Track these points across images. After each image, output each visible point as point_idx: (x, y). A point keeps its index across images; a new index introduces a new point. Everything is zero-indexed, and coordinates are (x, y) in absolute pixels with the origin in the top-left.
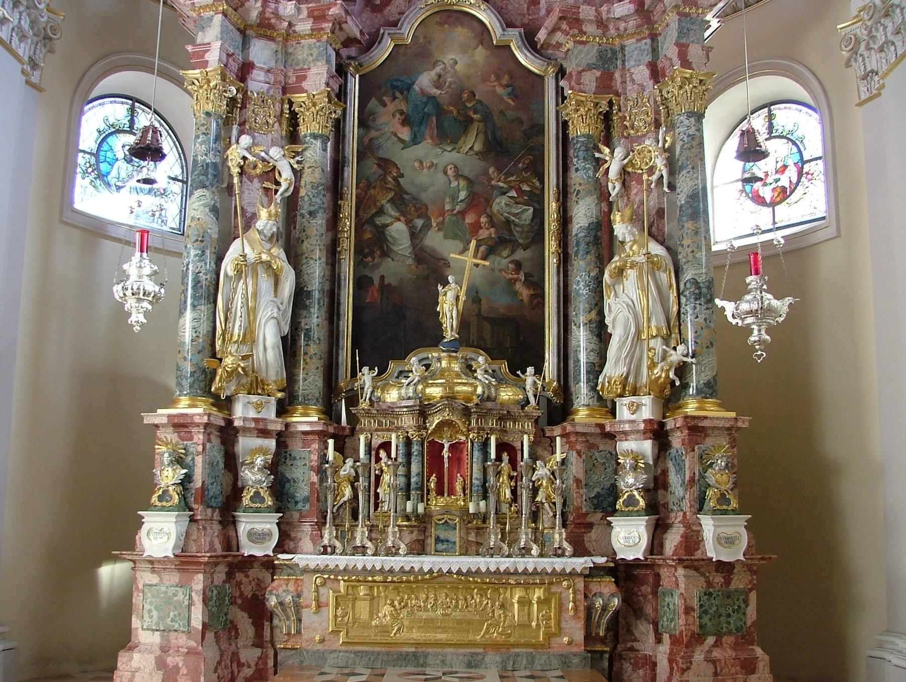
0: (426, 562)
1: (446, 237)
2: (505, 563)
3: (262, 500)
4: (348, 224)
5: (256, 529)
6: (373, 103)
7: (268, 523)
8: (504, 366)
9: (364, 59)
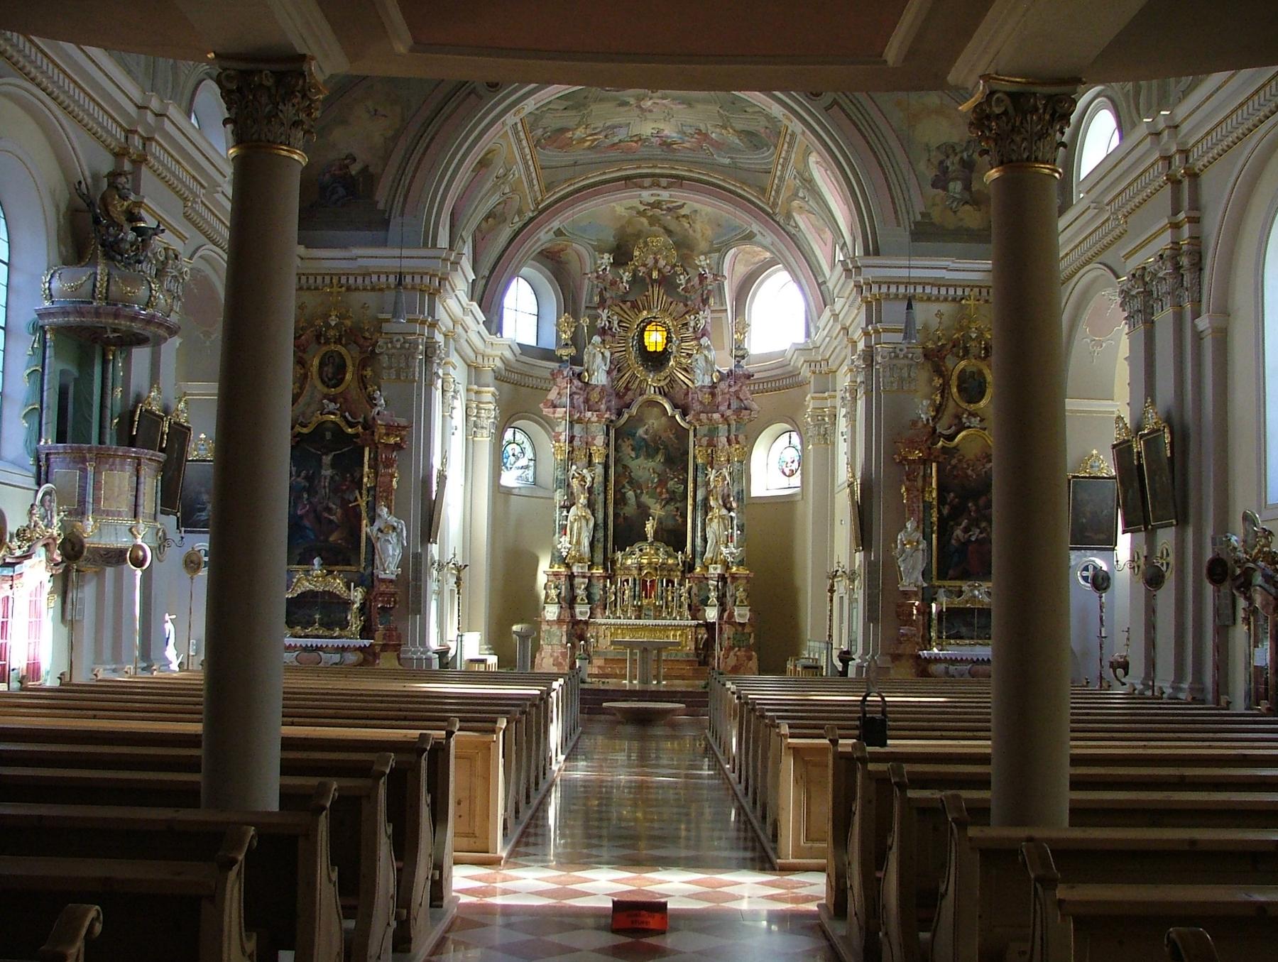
0: (641, 622)
2: (668, 622)
5: (582, 611)
7: (586, 608)
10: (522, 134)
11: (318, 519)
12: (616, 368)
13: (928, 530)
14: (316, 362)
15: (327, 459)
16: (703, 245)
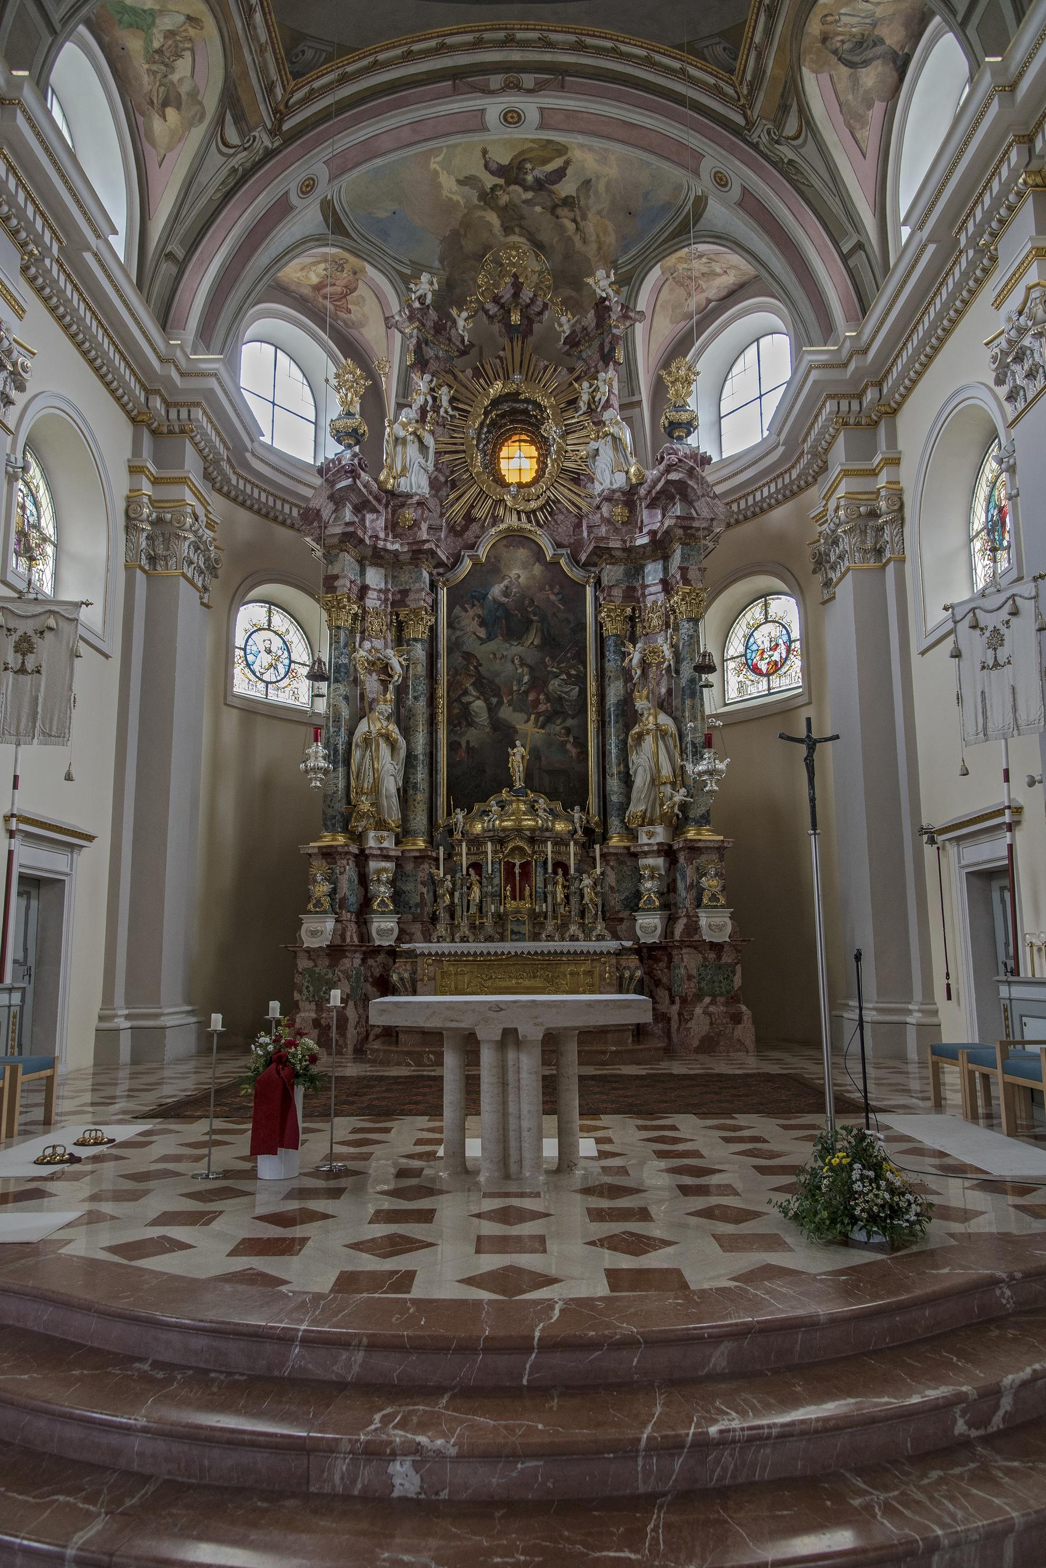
1: (514, 711)
3: (387, 906)
4: (442, 702)
5: (384, 927)
6: (457, 610)
8: (558, 806)
9: (449, 575)
12: (446, 481)
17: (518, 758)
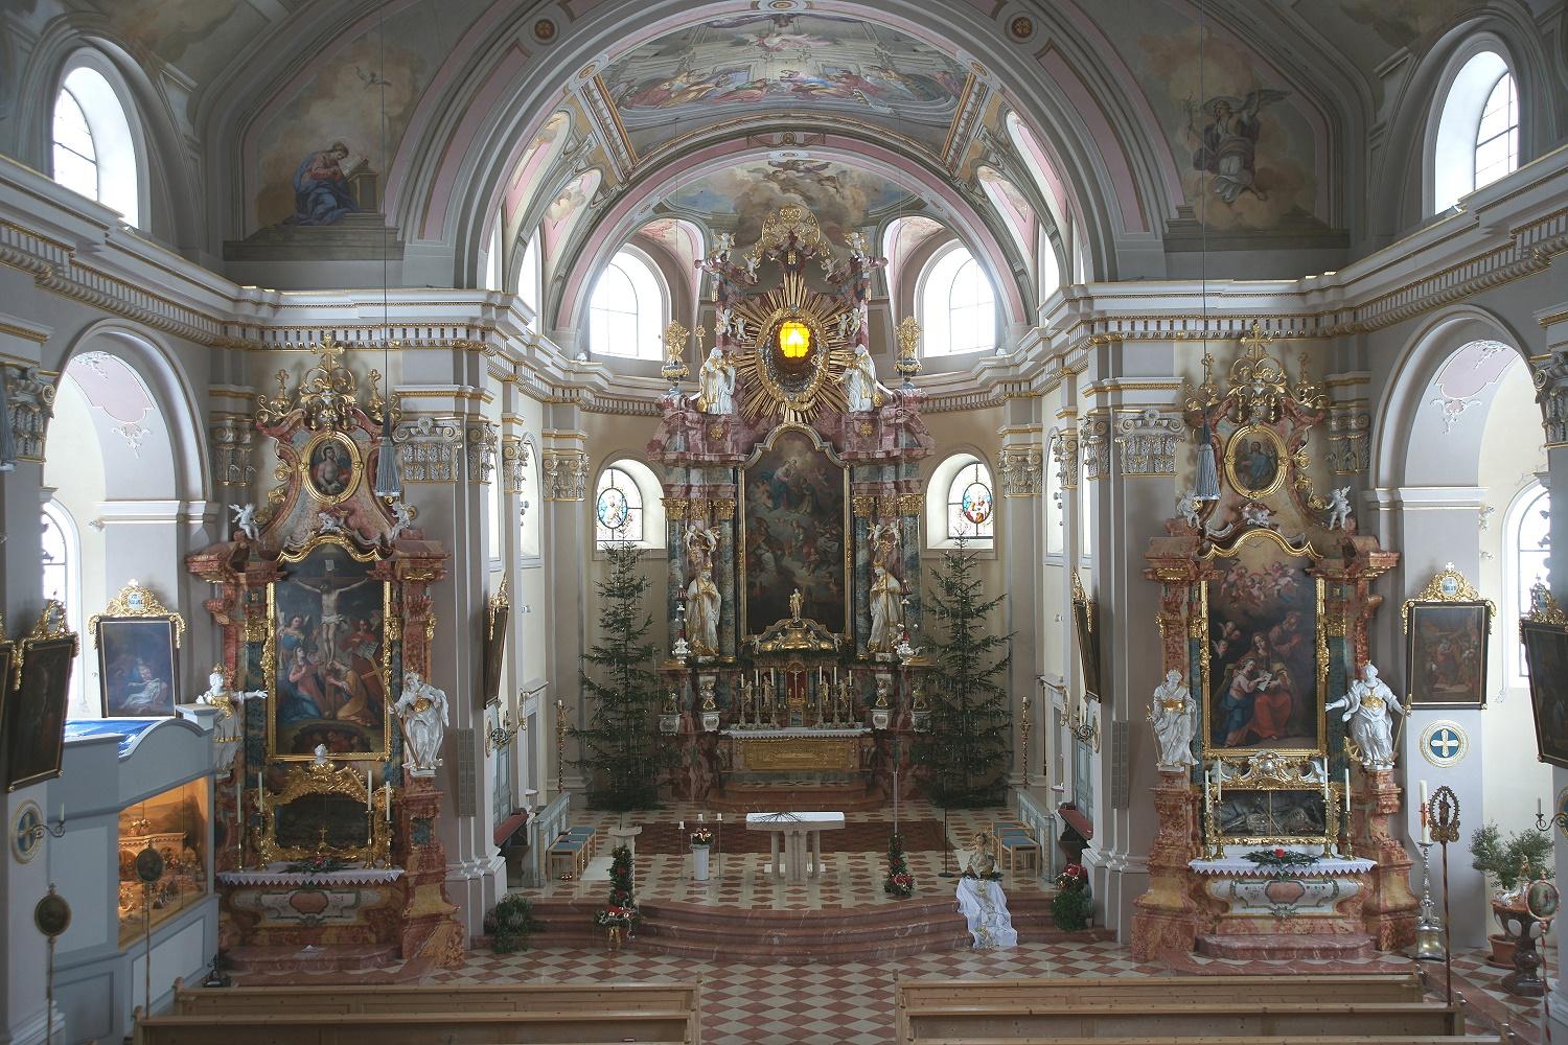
4: (743, 554)
5: (710, 719)
6: (752, 486)
10: (597, 95)
11: (320, 684)
12: (744, 390)
13: (1197, 680)
14: (306, 459)
15: (330, 600)
16: (855, 216)
17: (796, 601)
